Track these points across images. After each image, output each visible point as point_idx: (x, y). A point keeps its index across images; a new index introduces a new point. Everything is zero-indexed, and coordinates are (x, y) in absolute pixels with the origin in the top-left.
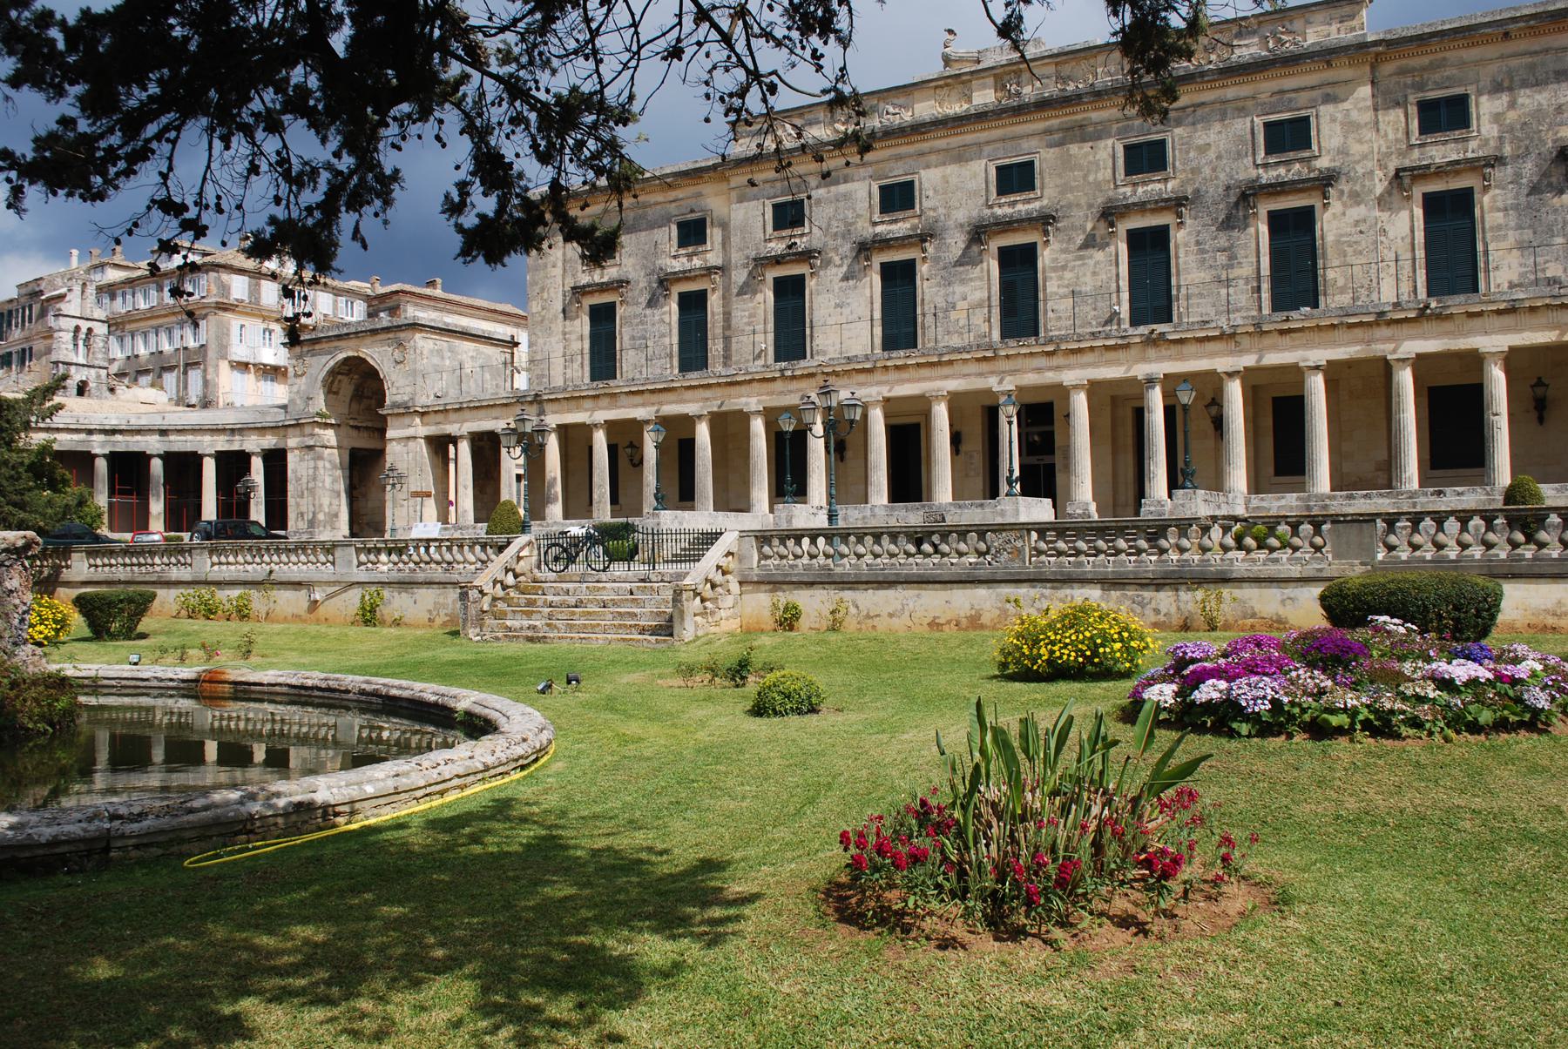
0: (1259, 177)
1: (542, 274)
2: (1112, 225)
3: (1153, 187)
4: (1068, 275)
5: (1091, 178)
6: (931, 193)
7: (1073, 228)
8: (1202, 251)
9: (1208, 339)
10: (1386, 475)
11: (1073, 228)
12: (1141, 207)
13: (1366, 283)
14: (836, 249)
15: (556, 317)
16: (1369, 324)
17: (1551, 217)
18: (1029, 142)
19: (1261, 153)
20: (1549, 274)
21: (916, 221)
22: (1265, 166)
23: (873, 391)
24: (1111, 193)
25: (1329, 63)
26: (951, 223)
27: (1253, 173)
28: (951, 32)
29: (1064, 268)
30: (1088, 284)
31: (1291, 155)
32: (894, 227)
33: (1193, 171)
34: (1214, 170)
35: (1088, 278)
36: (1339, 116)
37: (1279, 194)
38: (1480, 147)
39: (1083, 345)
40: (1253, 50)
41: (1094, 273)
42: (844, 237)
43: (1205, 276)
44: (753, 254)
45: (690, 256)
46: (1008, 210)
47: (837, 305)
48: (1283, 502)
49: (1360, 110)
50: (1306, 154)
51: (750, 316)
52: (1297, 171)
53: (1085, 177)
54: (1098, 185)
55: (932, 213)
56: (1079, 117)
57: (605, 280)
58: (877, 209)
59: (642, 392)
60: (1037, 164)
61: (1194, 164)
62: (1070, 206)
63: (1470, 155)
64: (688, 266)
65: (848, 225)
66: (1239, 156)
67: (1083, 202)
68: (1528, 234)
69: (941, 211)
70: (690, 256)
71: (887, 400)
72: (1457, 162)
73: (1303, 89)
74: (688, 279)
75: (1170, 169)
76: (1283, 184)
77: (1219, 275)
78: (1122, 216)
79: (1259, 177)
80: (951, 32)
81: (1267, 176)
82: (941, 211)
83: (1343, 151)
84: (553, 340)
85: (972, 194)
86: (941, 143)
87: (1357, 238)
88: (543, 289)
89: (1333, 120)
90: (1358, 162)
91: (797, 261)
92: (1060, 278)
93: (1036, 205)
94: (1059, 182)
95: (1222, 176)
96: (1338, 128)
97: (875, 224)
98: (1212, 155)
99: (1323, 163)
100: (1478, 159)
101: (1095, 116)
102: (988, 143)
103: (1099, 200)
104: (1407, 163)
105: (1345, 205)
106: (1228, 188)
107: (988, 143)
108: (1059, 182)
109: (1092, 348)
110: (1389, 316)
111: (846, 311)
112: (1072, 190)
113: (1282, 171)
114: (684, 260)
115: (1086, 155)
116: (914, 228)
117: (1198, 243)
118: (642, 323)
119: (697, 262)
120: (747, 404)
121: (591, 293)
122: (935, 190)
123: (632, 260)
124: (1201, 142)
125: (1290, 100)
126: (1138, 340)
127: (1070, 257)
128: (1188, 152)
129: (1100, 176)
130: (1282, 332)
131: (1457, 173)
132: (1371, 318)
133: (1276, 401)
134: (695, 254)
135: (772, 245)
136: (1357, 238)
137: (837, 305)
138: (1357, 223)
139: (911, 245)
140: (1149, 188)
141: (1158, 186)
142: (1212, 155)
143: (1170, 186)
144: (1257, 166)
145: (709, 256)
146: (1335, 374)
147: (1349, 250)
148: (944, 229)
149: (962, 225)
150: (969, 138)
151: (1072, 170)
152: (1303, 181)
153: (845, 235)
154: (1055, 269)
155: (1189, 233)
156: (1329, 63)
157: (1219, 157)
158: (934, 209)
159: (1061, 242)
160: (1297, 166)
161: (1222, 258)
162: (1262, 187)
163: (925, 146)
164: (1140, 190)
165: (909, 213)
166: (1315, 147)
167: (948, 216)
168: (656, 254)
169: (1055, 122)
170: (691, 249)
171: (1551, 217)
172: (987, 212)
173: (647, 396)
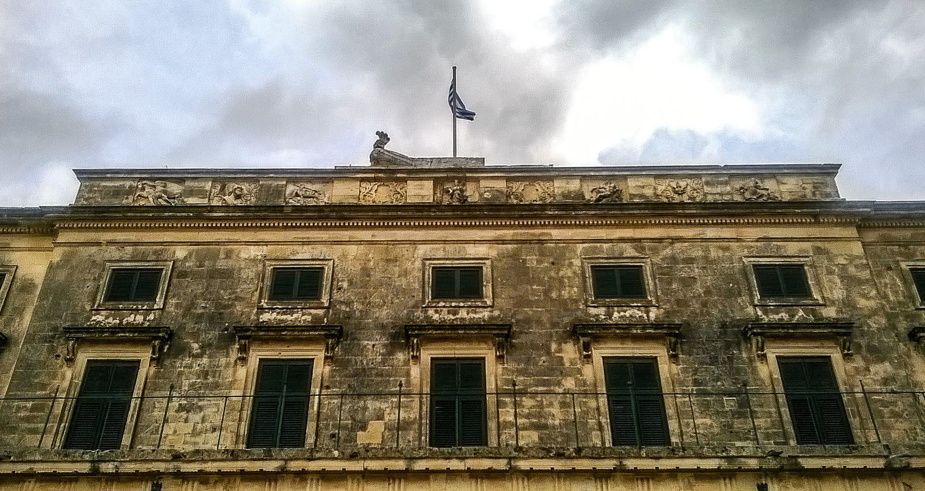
2: (587, 347)
4: (528, 402)
5: (554, 295)
7: (534, 347)
11: (534, 347)
12: (624, 332)
14: (195, 336)
18: (478, 246)
21: (321, 312)
24: (579, 313)
29: (523, 393)
30: (556, 415)
33: (678, 302)
34: (704, 304)
35: (555, 410)
41: (563, 405)
49: (856, 266)
51: (33, 409)
53: (547, 293)
54: (563, 303)
55: (343, 308)
58: (266, 294)
61: (681, 295)
62: (528, 321)
65: (218, 305)
66: (731, 294)
67: (545, 318)
69: (356, 305)
73: (791, 239)
78: (597, 339)
83: (847, 303)
86: (366, 235)
89: (830, 272)
90: (869, 317)
91: (133, 342)
93: (485, 314)
94: (513, 293)
95: (714, 312)
98: (699, 289)
99: (830, 313)
101: (556, 233)
102: (425, 242)
103: (566, 320)
105: (865, 359)
106: (724, 326)
107: (425, 242)
108: (513, 293)
111: (195, 417)
112: (529, 304)
115: (546, 270)
117: (696, 383)
122: (351, 283)
125: (779, 248)
127: (530, 380)
128: (670, 283)
129: (565, 294)
142: (699, 289)
144: (755, 306)
148: (360, 327)
149: (383, 327)
150: (400, 235)
151: (530, 283)
153: (213, 319)
155: (684, 370)
157: (708, 292)
158: (348, 303)
159: (518, 362)
161: (730, 403)
163: (345, 235)
165: (314, 303)
167: (365, 313)
169: (508, 233)
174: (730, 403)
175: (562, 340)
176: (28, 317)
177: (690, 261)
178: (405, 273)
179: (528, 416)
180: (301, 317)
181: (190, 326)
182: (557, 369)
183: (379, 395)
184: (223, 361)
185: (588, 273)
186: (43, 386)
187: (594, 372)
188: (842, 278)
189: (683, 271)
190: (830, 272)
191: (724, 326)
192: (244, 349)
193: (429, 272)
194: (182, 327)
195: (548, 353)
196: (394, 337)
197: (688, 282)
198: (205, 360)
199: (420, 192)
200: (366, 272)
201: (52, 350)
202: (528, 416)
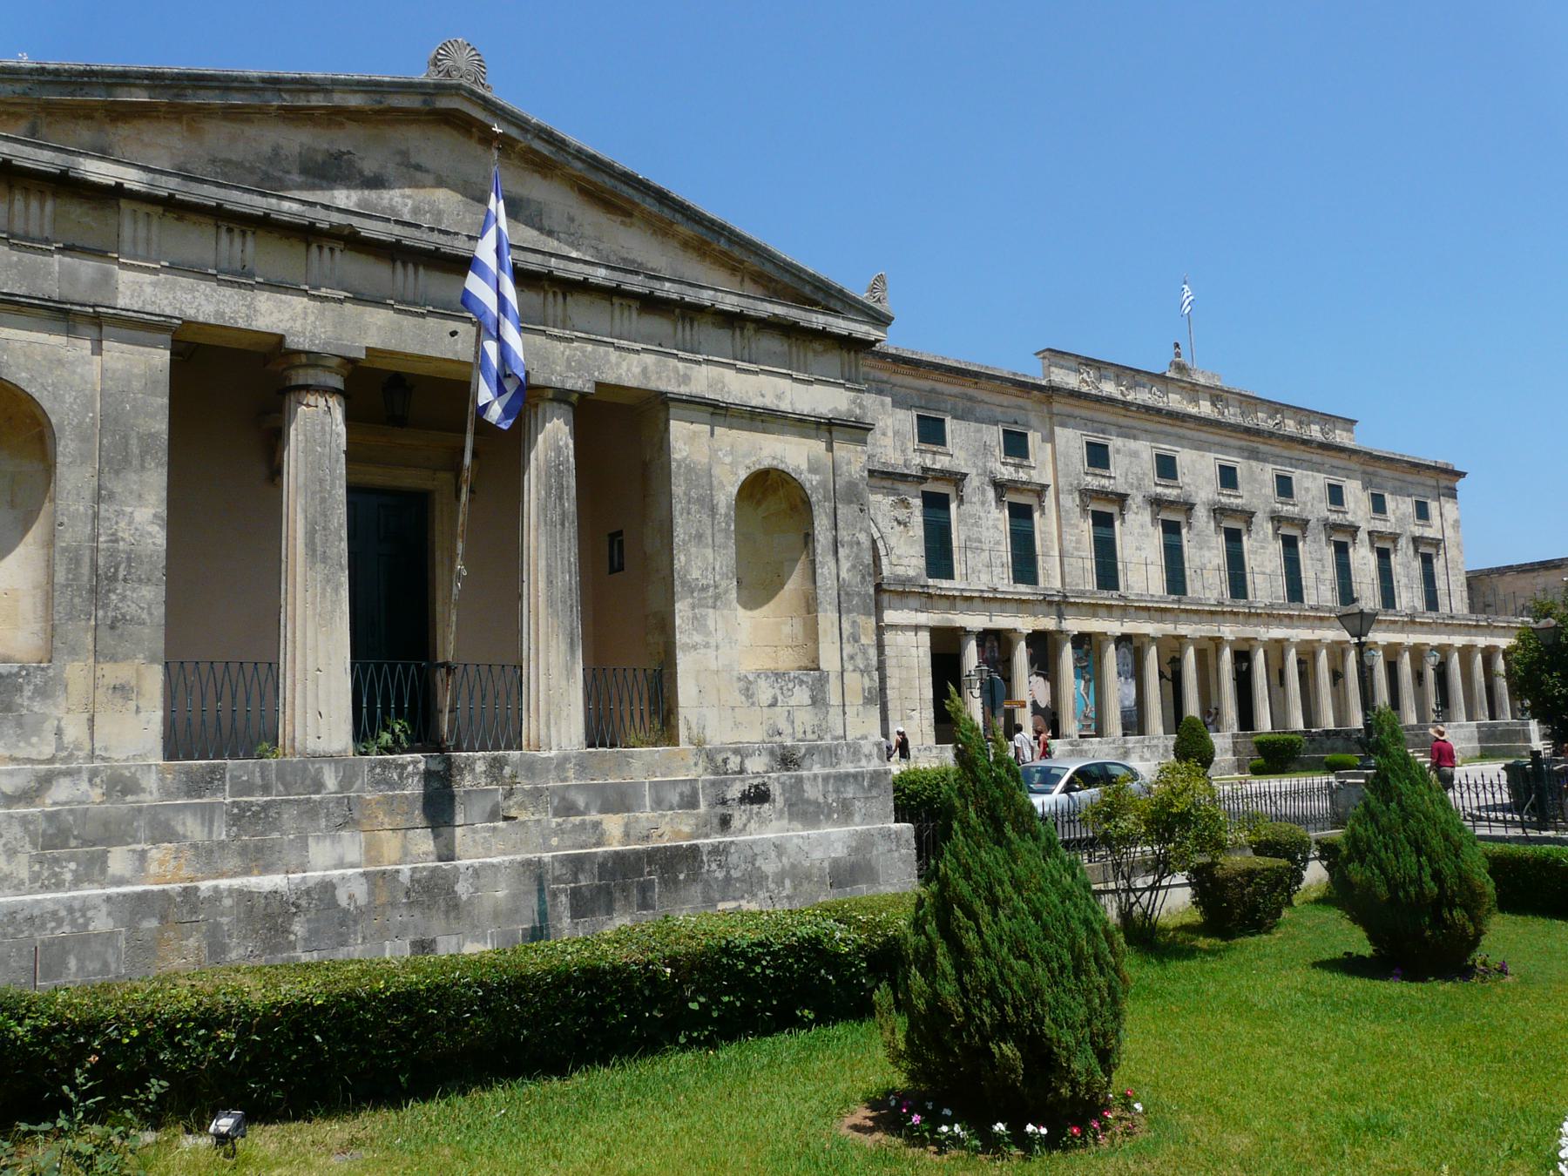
57: (937, 466)
64: (1015, 476)
93: (1238, 501)
99: (1349, 517)
114: (1012, 469)
116: (1178, 496)
135: (1089, 478)
139: (1179, 511)
169: (1244, 443)
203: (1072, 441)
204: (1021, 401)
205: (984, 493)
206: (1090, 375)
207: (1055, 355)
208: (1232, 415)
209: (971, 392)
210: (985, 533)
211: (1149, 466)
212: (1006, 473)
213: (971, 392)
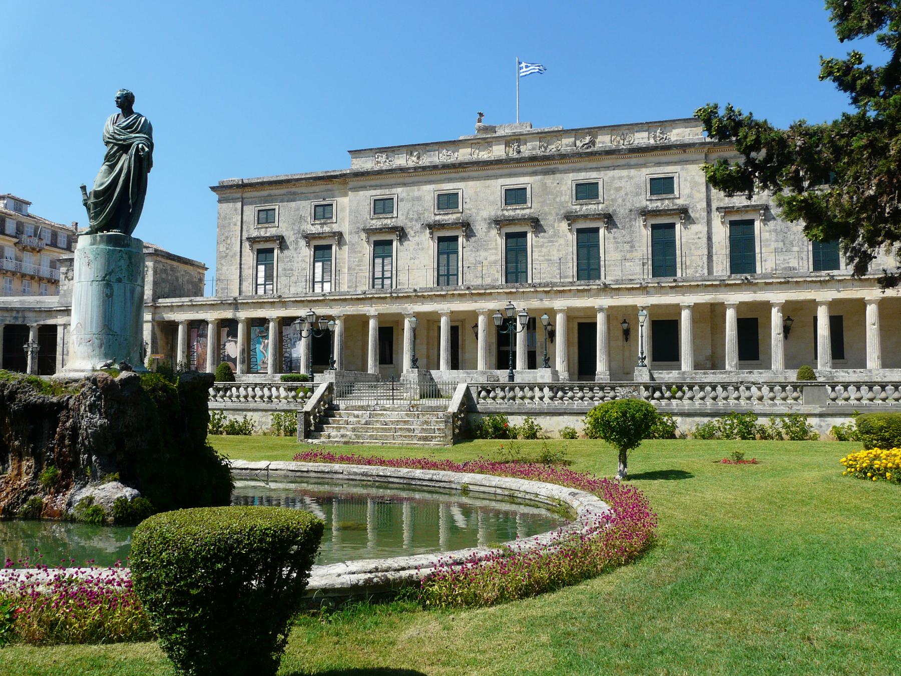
0: (647, 206)
1: (227, 229)
3: (591, 208)
4: (544, 250)
5: (558, 200)
6: (468, 201)
8: (617, 243)
9: (633, 289)
10: (714, 362)
12: (585, 217)
13: (701, 264)
14: (411, 228)
15: (235, 254)
16: (716, 285)
17: (792, 237)
19: (649, 194)
20: (791, 265)
21: (459, 215)
22: (651, 200)
23: (371, 310)
25: (685, 151)
26: (479, 218)
27: (645, 203)
28: (481, 114)
29: (542, 246)
31: (664, 196)
32: (446, 217)
33: (612, 200)
34: (624, 200)
35: (555, 252)
36: (689, 178)
37: (657, 215)
38: (758, 199)
39: (565, 288)
40: (646, 141)
41: (558, 250)
42: (416, 221)
43: (617, 256)
44: (362, 227)
45: (322, 224)
46: (512, 213)
47: (411, 259)
48: (671, 375)
50: (671, 196)
52: (666, 204)
53: (554, 199)
54: (561, 204)
56: (553, 166)
57: (268, 235)
59: (303, 301)
60: (529, 190)
61: (613, 197)
62: (546, 214)
63: (753, 203)
64: (320, 230)
65: (419, 214)
66: (638, 194)
67: (553, 212)
68: (781, 245)
70: (322, 224)
71: (452, 312)
72: (748, 206)
74: (320, 238)
75: (601, 199)
76: (659, 211)
77: (625, 255)
79: (647, 206)
80: (481, 114)
81: (652, 206)
82: (474, 210)
83: (690, 196)
84: (233, 268)
85: (493, 203)
87: (696, 240)
88: (227, 238)
89: (686, 180)
92: (540, 252)
93: (527, 211)
94: (540, 199)
95: (628, 204)
96: (688, 184)
97: (435, 215)
98: (622, 193)
99: (680, 202)
100: (758, 206)
104: (722, 205)
109: (570, 290)
110: (727, 282)
111: (417, 262)
113: (659, 204)
114: (318, 227)
116: (458, 219)
117: (614, 238)
118: (290, 261)
119: (326, 229)
120: (368, 311)
121: (259, 242)
123: (285, 225)
124: (617, 186)
126: (595, 287)
127: (545, 240)
128: (610, 190)
130: (671, 287)
131: (747, 211)
132: (717, 283)
133: (580, 325)
134: (325, 223)
135: (374, 222)
136: (696, 240)
137: (411, 259)
138: (697, 233)
139: (458, 228)
140: (590, 206)
141: (594, 207)
142: (622, 193)
143: (601, 206)
145: (334, 225)
146: (696, 309)
147: (693, 247)
149: (485, 219)
151: (547, 194)
152: (671, 210)
154: (537, 247)
156: (685, 151)
157: (626, 194)
158: (469, 209)
160: (667, 202)
161: (627, 247)
162: (649, 212)
164: (584, 208)
165: (456, 210)
166: (676, 193)
167: (477, 214)
168: (300, 222)
170: (322, 221)
171: (792, 237)
172: (500, 213)
173: (306, 303)
174: (627, 247)
175: (560, 221)
176: (347, 223)
177: (621, 178)
178: (493, 193)
179: (544, 256)
180: (451, 218)
181: (409, 224)
182: (556, 234)
183: (486, 250)
184: (424, 238)
185: (574, 188)
186: (360, 252)
187: (572, 238)
188: (690, 182)
189: (617, 184)
190: (686, 180)
191: (631, 211)
192: (431, 233)
193: (503, 192)
194: (406, 224)
195: (554, 227)
196: (489, 224)
197: (618, 189)
198: (417, 238)
199: (498, 151)
200: (476, 193)
201: (359, 237)
202: (544, 256)
203: (306, 207)
204: (329, 187)
205: (297, 243)
206: (383, 158)
207: (355, 153)
208: (527, 150)
209: (294, 190)
210: (295, 264)
211: (431, 203)
212: (316, 229)
213: (294, 190)
